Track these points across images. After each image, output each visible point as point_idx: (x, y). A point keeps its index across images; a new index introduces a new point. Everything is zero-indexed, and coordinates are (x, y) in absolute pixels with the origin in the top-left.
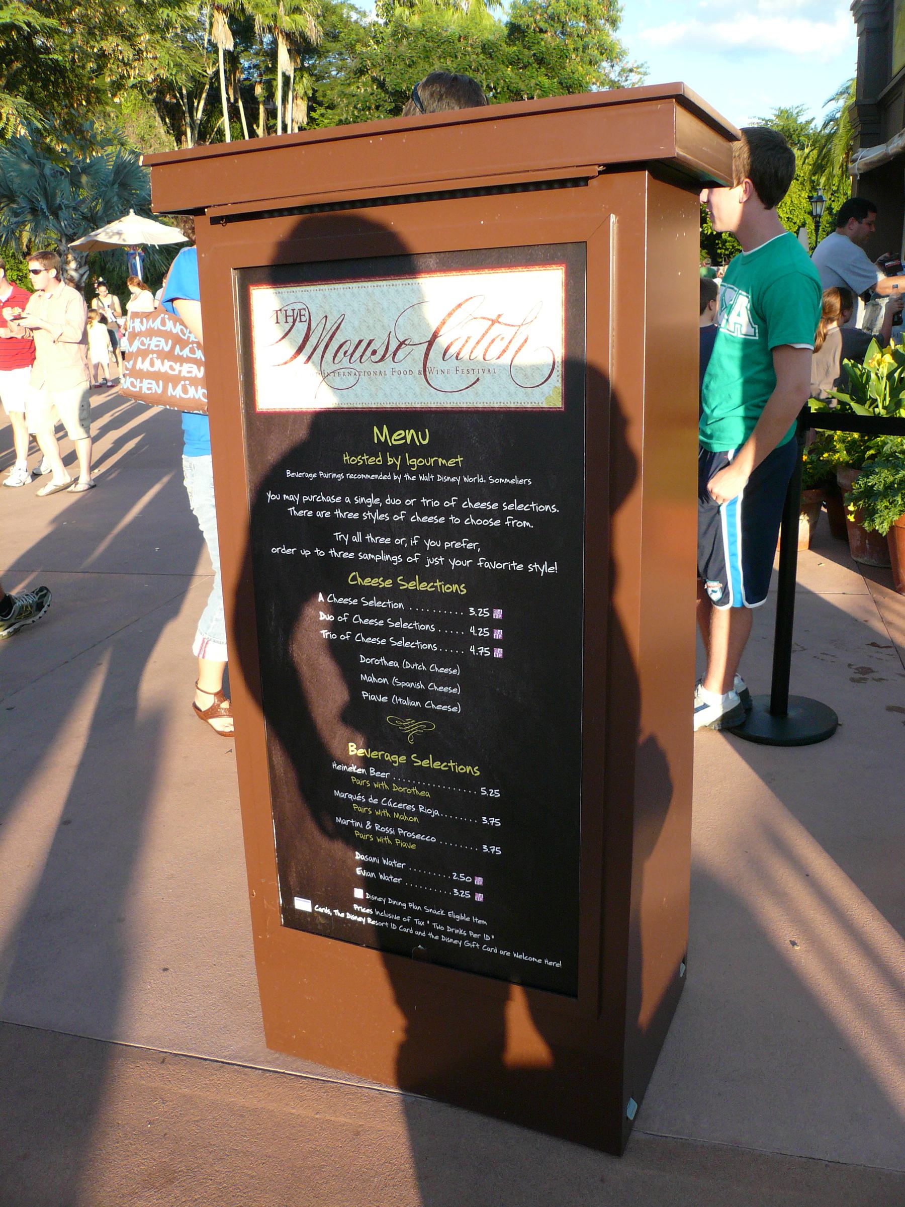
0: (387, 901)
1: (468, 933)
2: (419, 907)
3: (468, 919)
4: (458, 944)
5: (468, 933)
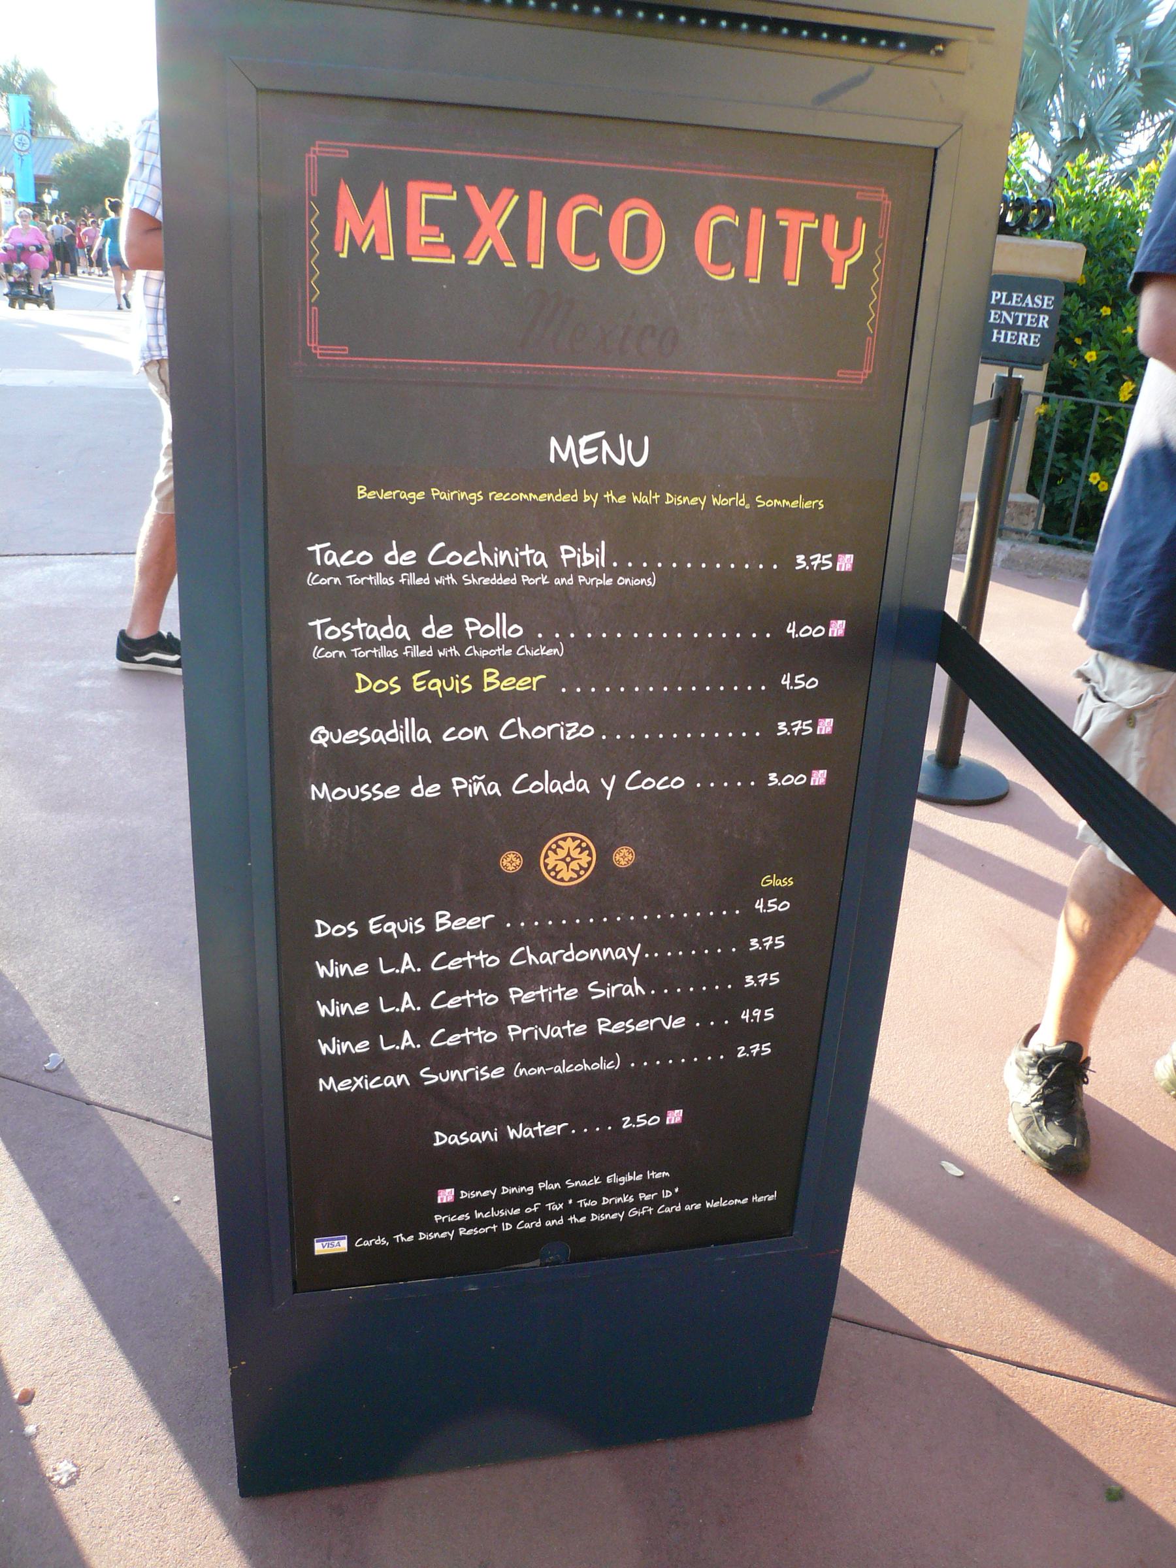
0: (500, 1190)
1: (636, 1197)
2: (557, 1185)
3: (639, 1178)
4: (619, 1218)
5: (636, 1197)
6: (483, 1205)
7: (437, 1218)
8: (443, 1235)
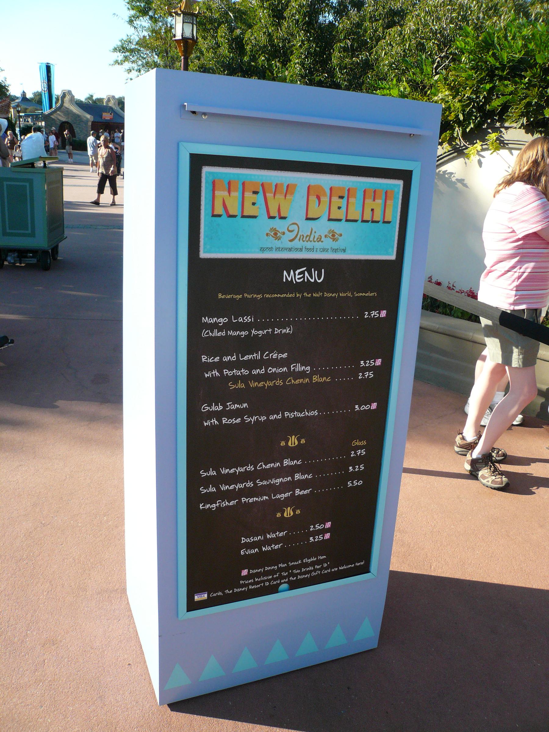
1: (314, 568)
5: (314, 568)
6: (258, 575)
7: (241, 582)
8: (243, 589)
